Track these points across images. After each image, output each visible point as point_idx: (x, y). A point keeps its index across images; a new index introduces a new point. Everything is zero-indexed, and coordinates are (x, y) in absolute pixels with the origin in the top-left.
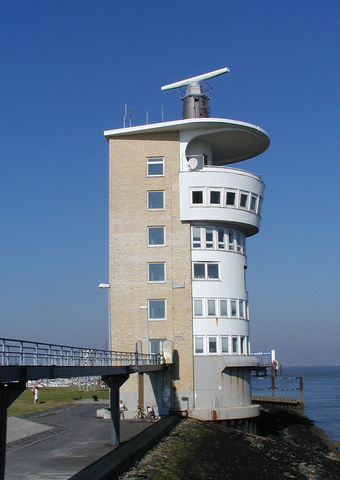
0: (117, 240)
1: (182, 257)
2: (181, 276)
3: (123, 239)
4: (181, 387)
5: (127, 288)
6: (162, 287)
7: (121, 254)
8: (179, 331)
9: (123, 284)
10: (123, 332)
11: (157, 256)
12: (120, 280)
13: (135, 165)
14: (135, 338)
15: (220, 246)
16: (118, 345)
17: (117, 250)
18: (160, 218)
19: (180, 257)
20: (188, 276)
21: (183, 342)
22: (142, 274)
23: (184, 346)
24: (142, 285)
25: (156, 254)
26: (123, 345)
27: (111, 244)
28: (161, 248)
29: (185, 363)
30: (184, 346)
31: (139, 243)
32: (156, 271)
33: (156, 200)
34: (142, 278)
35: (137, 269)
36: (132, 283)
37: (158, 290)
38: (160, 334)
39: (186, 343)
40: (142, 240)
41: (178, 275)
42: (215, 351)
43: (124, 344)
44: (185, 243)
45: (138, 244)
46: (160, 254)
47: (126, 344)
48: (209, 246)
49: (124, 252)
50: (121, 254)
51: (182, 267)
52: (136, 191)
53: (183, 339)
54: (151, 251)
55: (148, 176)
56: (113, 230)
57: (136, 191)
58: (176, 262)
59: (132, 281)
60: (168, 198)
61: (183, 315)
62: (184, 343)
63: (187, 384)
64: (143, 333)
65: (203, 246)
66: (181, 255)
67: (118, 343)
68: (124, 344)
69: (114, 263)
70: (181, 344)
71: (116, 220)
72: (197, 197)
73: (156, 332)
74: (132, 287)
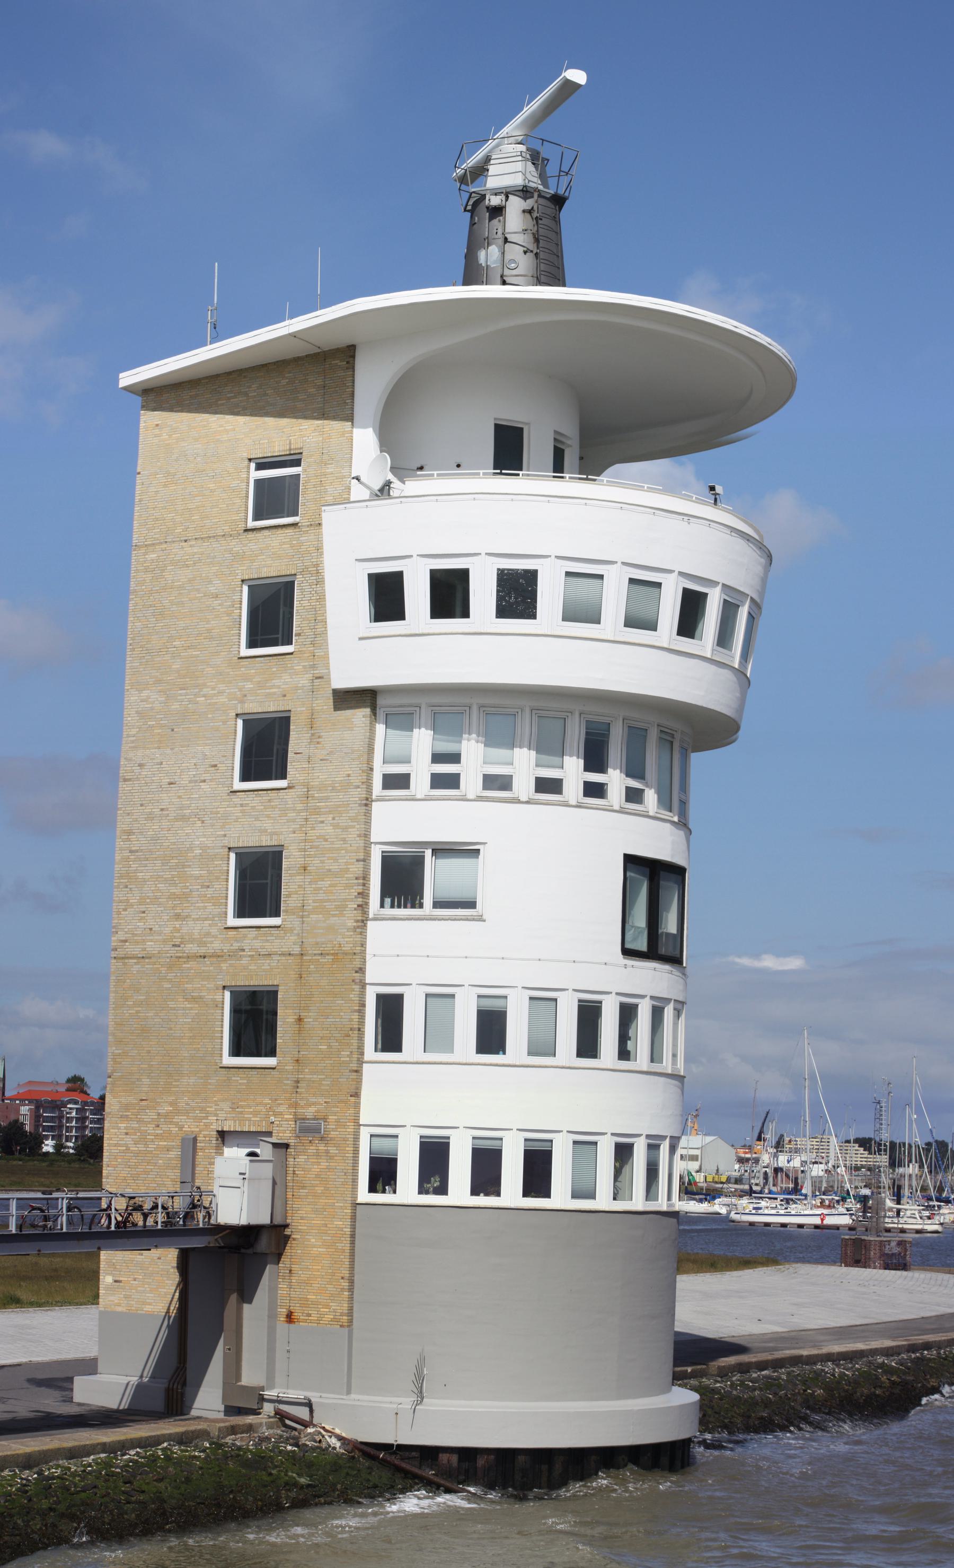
0: (141, 765)
1: (336, 826)
2: (329, 900)
3: (161, 763)
4: (309, 1315)
5: (165, 941)
6: (267, 941)
7: (150, 817)
8: (312, 1109)
9: (151, 929)
10: (144, 1103)
11: (258, 824)
12: (144, 912)
13: (212, 486)
14: (176, 1124)
15: (438, 781)
16: (128, 1149)
17: (142, 805)
18: (276, 682)
19: (330, 830)
20: (351, 900)
21: (322, 1147)
22: (210, 891)
23: (324, 1164)
24: (208, 934)
25: (257, 819)
26: (141, 1147)
27: (125, 780)
28: (273, 794)
29: (326, 1225)
30: (324, 1164)
31: (207, 776)
32: (259, 883)
33: (272, 614)
34: (210, 907)
35: (196, 872)
36: (177, 924)
37: (261, 951)
38: (255, 1114)
39: (333, 1150)
40: (215, 766)
41: (321, 896)
42: (442, 1190)
43: (146, 1145)
44: (349, 776)
45: (204, 781)
46: (268, 816)
47: (152, 1147)
48: (594, 790)
49: (162, 810)
50: (150, 817)
51: (334, 867)
52: (210, 582)
53: (322, 1139)
54: (242, 805)
55: (251, 524)
56: (134, 731)
57: (210, 582)
58: (317, 847)
59: (178, 917)
60: (306, 603)
61: (330, 1046)
62: (327, 1152)
63: (328, 1306)
64: (202, 1110)
65: (420, 783)
66: (334, 819)
67: (128, 1140)
68: (146, 1145)
69: (131, 851)
70: (318, 1155)
71: (145, 694)
72: (386, 597)
73: (242, 1107)
74: (177, 941)
